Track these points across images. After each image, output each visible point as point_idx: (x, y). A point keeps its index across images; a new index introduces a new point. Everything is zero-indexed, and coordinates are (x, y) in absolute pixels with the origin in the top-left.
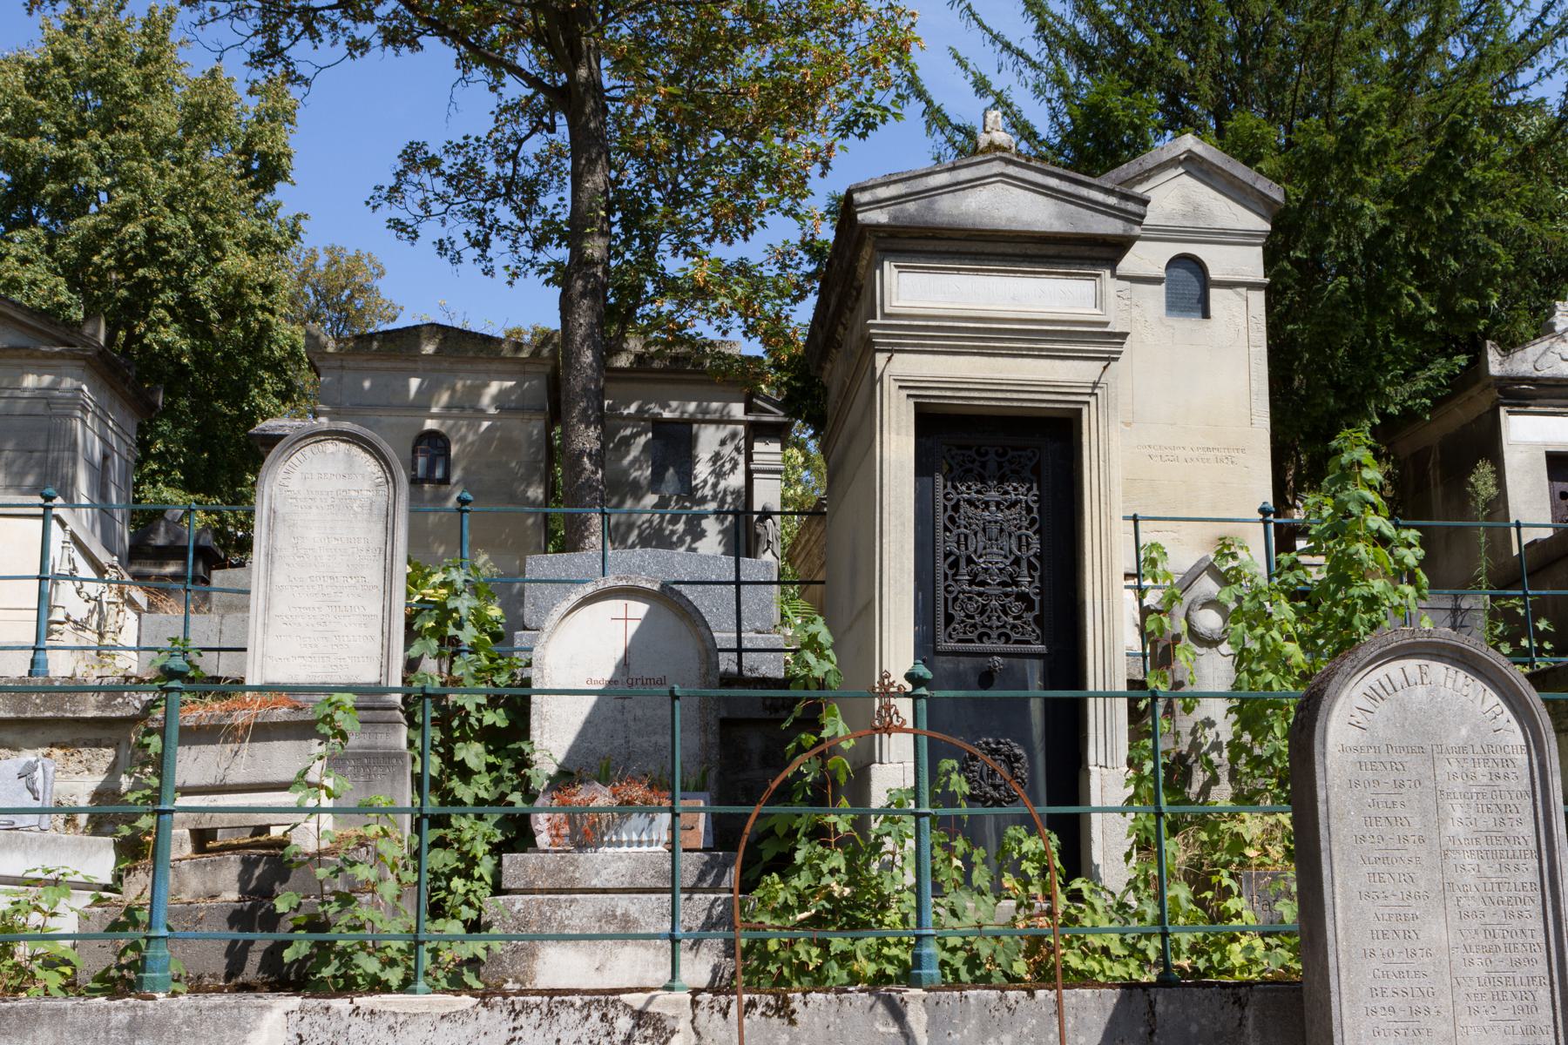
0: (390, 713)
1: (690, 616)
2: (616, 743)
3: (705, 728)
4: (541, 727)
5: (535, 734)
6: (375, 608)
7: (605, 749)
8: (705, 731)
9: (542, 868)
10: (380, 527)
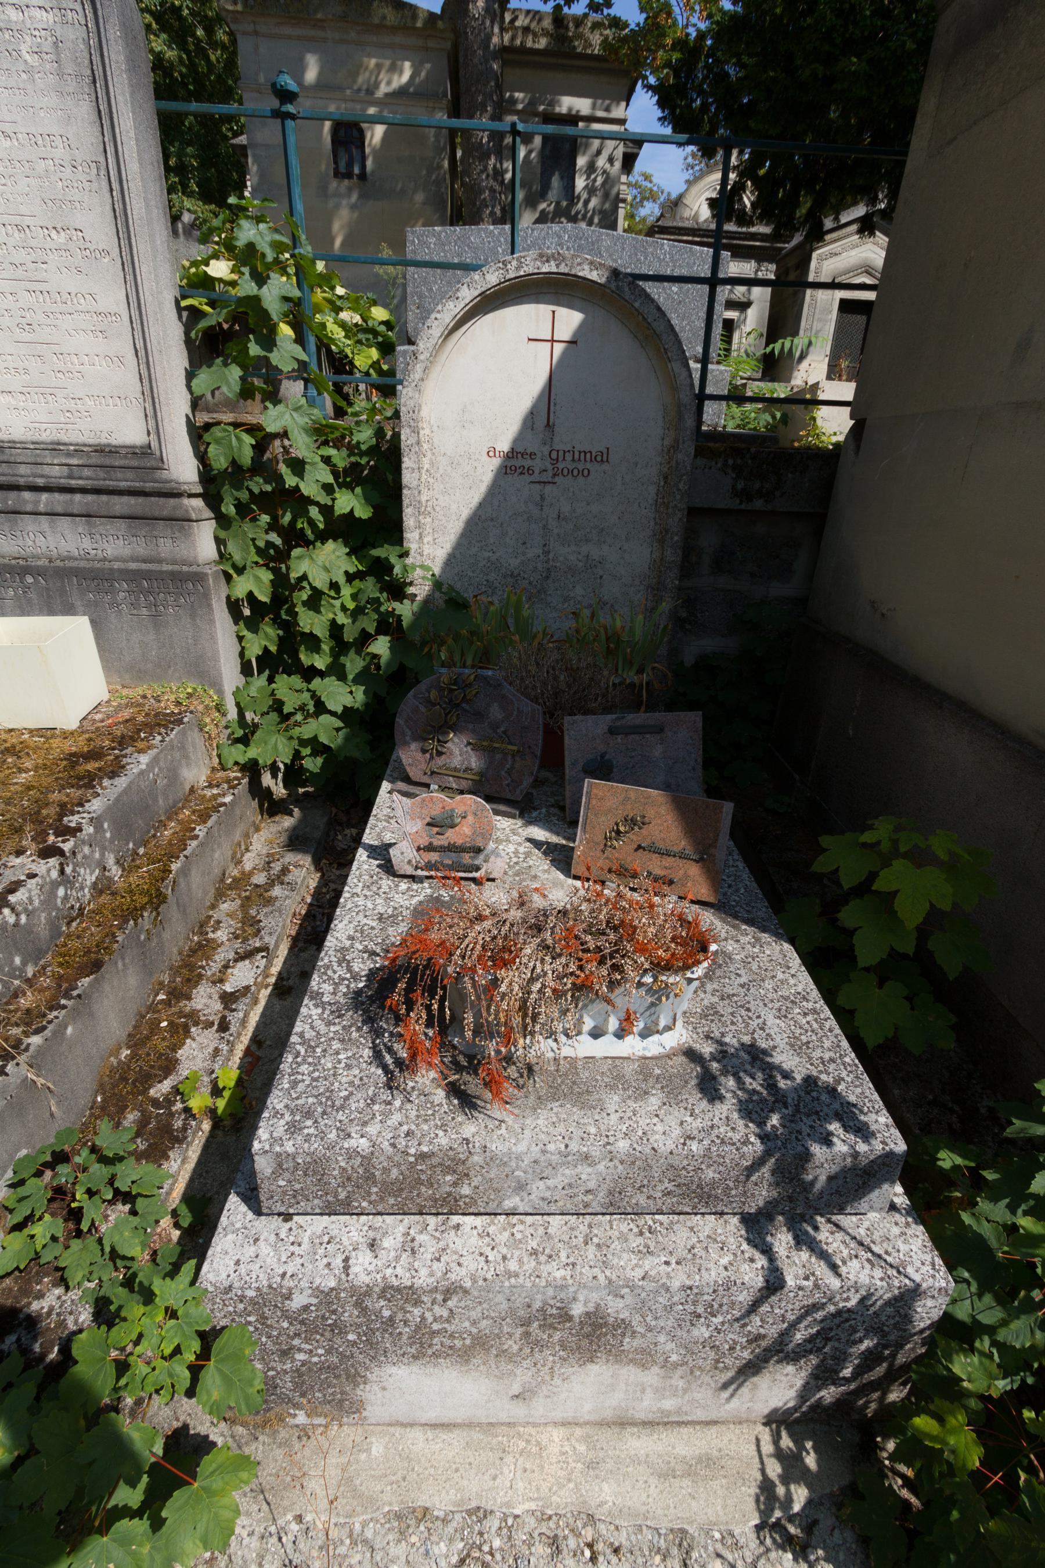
0: (172, 501)
1: (653, 333)
2: (531, 553)
3: (661, 537)
4: (419, 526)
5: (411, 537)
6: (112, 297)
7: (514, 563)
8: (662, 542)
9: (370, 1178)
10: (84, 109)
